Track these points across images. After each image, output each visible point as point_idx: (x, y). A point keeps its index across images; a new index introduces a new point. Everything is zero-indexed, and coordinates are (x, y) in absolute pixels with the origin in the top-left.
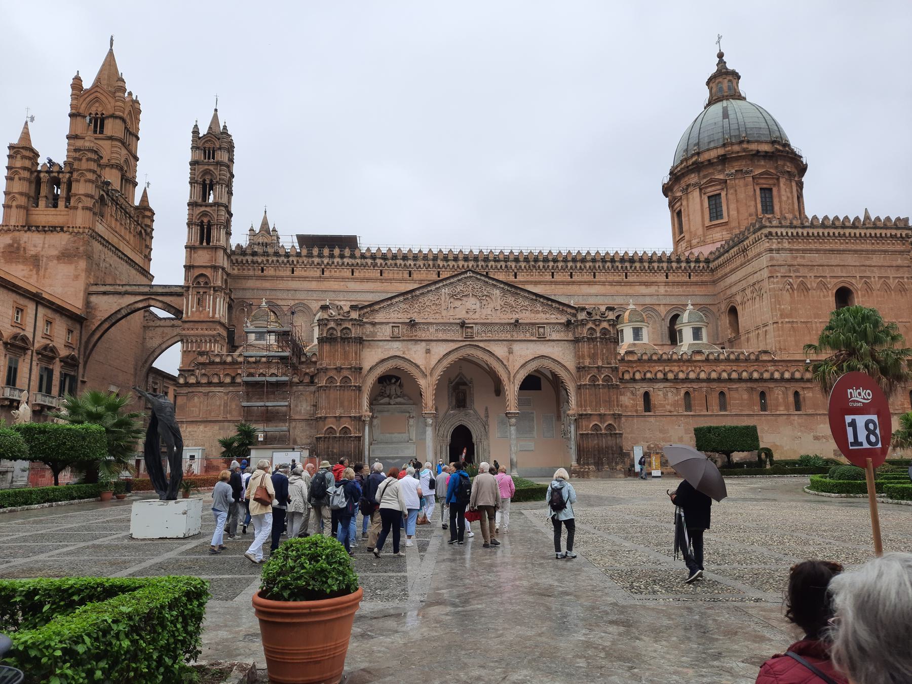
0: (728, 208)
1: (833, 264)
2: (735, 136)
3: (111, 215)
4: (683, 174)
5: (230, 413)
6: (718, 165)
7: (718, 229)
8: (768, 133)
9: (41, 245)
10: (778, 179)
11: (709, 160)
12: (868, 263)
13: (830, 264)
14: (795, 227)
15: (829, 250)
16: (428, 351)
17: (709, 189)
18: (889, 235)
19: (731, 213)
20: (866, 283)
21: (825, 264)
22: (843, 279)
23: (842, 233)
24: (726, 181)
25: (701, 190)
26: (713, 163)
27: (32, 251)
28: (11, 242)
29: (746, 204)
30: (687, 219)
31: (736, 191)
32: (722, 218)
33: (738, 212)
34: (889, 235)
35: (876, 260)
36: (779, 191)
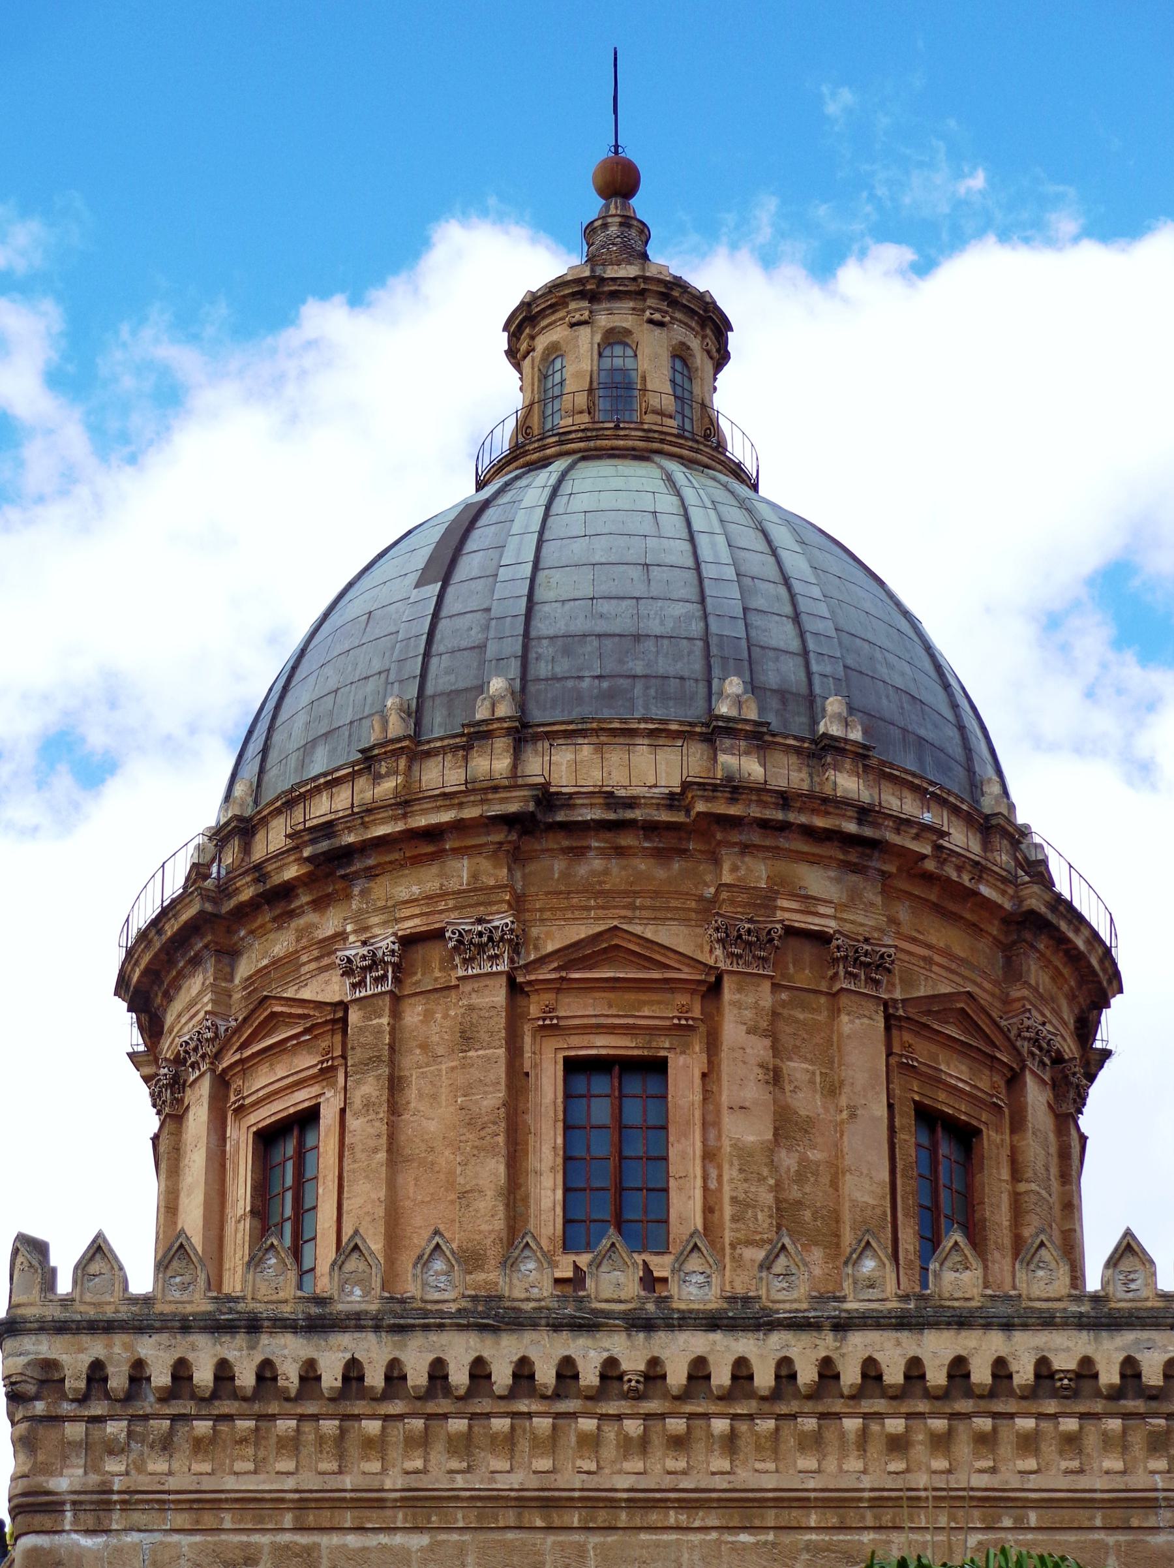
6: (321, 904)
8: (698, 666)
10: (713, 990)
14: (253, 1326)
15: (521, 1502)
17: (263, 1079)
18: (1023, 1373)
23: (633, 1361)
26: (286, 891)
34: (1023, 1373)
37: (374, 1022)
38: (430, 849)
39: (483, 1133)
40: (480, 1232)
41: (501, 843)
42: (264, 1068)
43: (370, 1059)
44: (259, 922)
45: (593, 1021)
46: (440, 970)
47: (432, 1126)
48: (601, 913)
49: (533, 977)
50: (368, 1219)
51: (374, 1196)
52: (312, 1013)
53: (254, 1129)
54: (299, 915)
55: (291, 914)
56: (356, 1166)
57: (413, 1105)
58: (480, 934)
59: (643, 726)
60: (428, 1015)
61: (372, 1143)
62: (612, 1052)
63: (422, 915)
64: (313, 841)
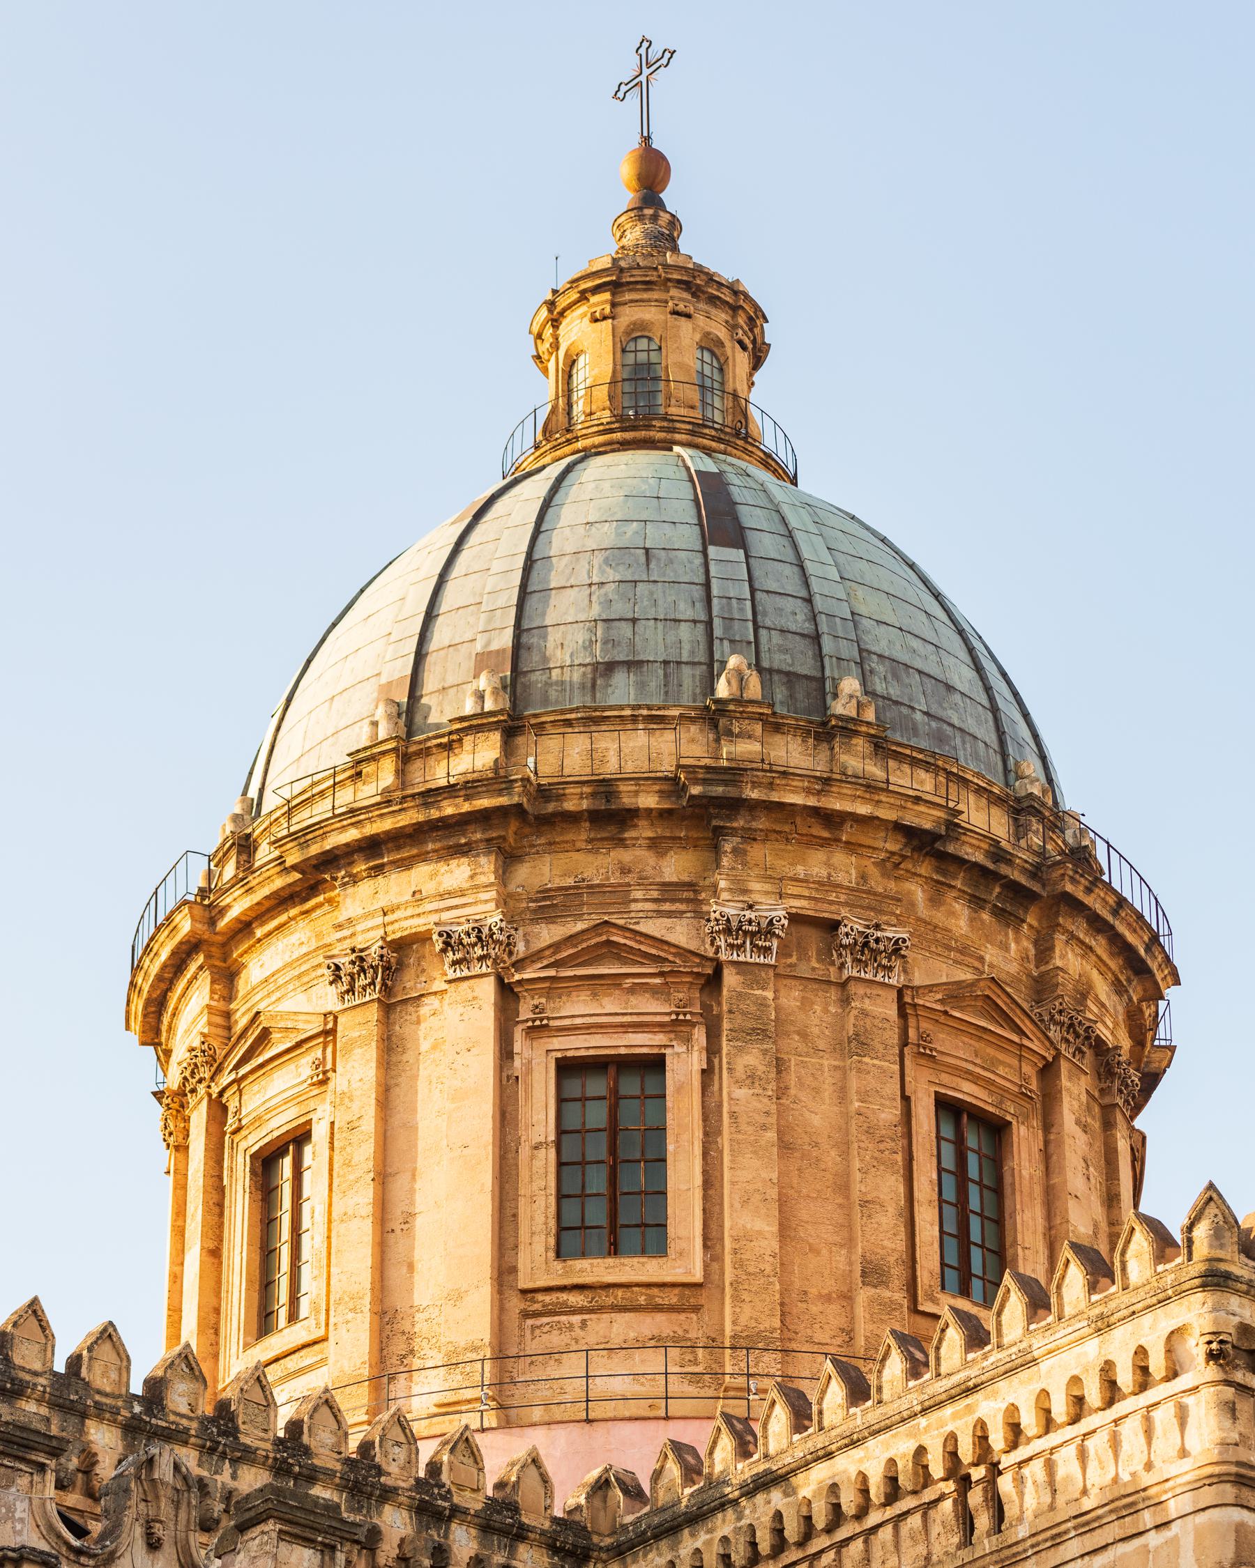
0: (710, 1183)
2: (791, 678)
4: (371, 846)
7: (622, 1327)
10: (1048, 1071)
11: (605, 787)
17: (577, 1007)
19: (734, 1220)
24: (713, 981)
25: (507, 993)
26: (628, 817)
29: (843, 1187)
30: (362, 1198)
31: (780, 1065)
32: (660, 1249)
33: (785, 1231)
36: (1049, 1156)
37: (756, 992)
38: (826, 834)
39: (882, 1146)
40: (883, 1248)
41: (893, 853)
42: (584, 996)
43: (753, 1029)
44: (569, 837)
45: (964, 1064)
46: (819, 961)
47: (816, 1121)
48: (960, 957)
49: (921, 1002)
50: (758, 1197)
51: (765, 1175)
52: (670, 958)
53: (559, 1055)
54: (626, 847)
55: (621, 843)
56: (740, 1137)
57: (793, 1092)
58: (877, 940)
59: (976, 780)
60: (805, 1004)
61: (762, 1119)
62: (974, 1101)
63: (810, 898)
64: (705, 782)
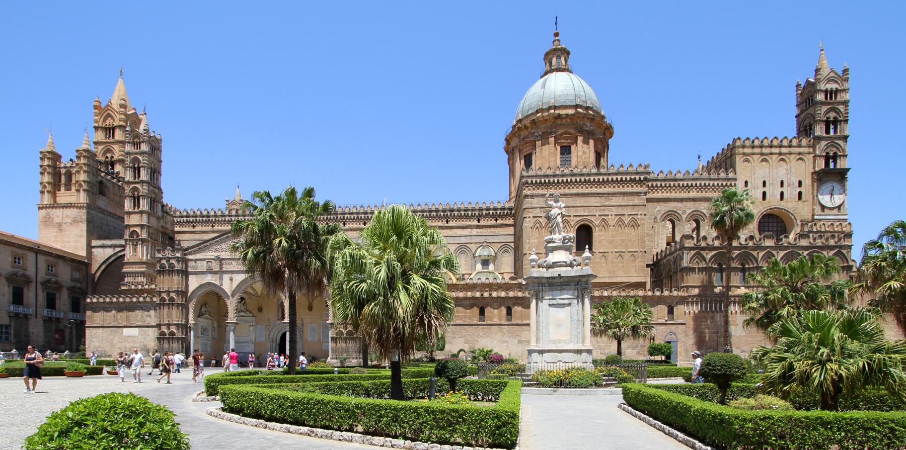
1: (578, 205)
3: (114, 194)
5: (117, 321)
9: (61, 216)
12: (607, 203)
13: (575, 205)
16: (231, 279)
20: (604, 220)
21: (571, 205)
22: (585, 217)
27: (57, 220)
28: (45, 215)
35: (615, 201)
